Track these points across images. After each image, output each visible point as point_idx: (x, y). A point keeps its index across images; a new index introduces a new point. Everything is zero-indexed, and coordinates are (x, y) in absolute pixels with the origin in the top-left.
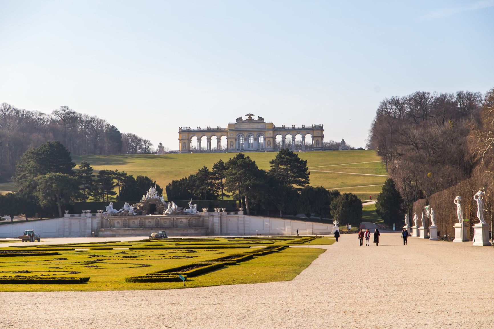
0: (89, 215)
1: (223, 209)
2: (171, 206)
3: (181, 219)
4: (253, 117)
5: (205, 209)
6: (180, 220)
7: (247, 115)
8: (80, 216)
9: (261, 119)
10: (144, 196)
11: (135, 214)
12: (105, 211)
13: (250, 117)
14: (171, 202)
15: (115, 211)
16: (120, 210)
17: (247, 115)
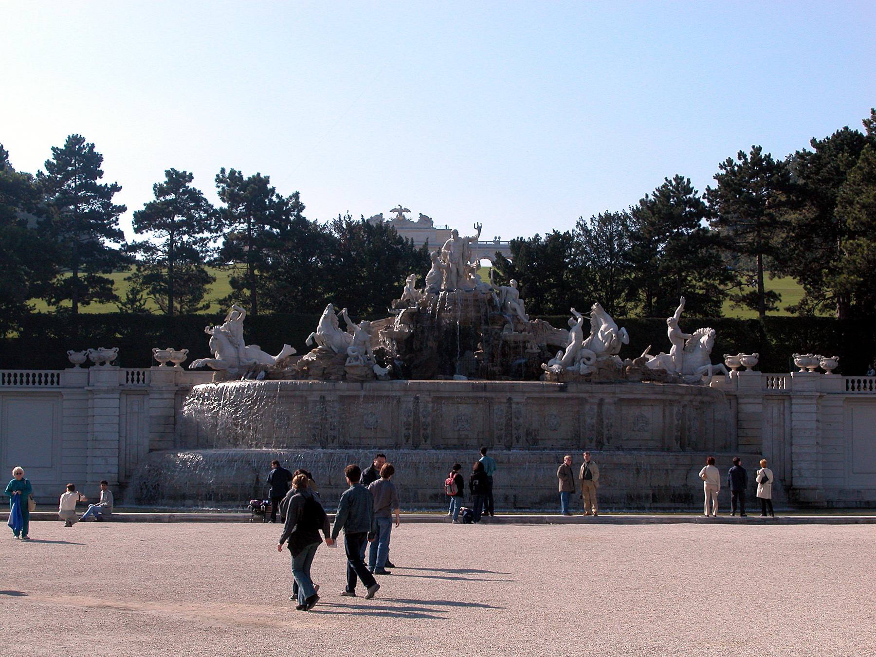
0: (109, 376)
1: (824, 362)
2: (586, 329)
3: (638, 402)
4: (407, 216)
5: (743, 358)
6: (633, 411)
7: (393, 211)
8: (55, 381)
9: (425, 220)
10: (410, 281)
11: (378, 369)
12: (200, 348)
13: (400, 214)
14: (585, 309)
15: (255, 354)
16: (288, 349)
17: (393, 211)
